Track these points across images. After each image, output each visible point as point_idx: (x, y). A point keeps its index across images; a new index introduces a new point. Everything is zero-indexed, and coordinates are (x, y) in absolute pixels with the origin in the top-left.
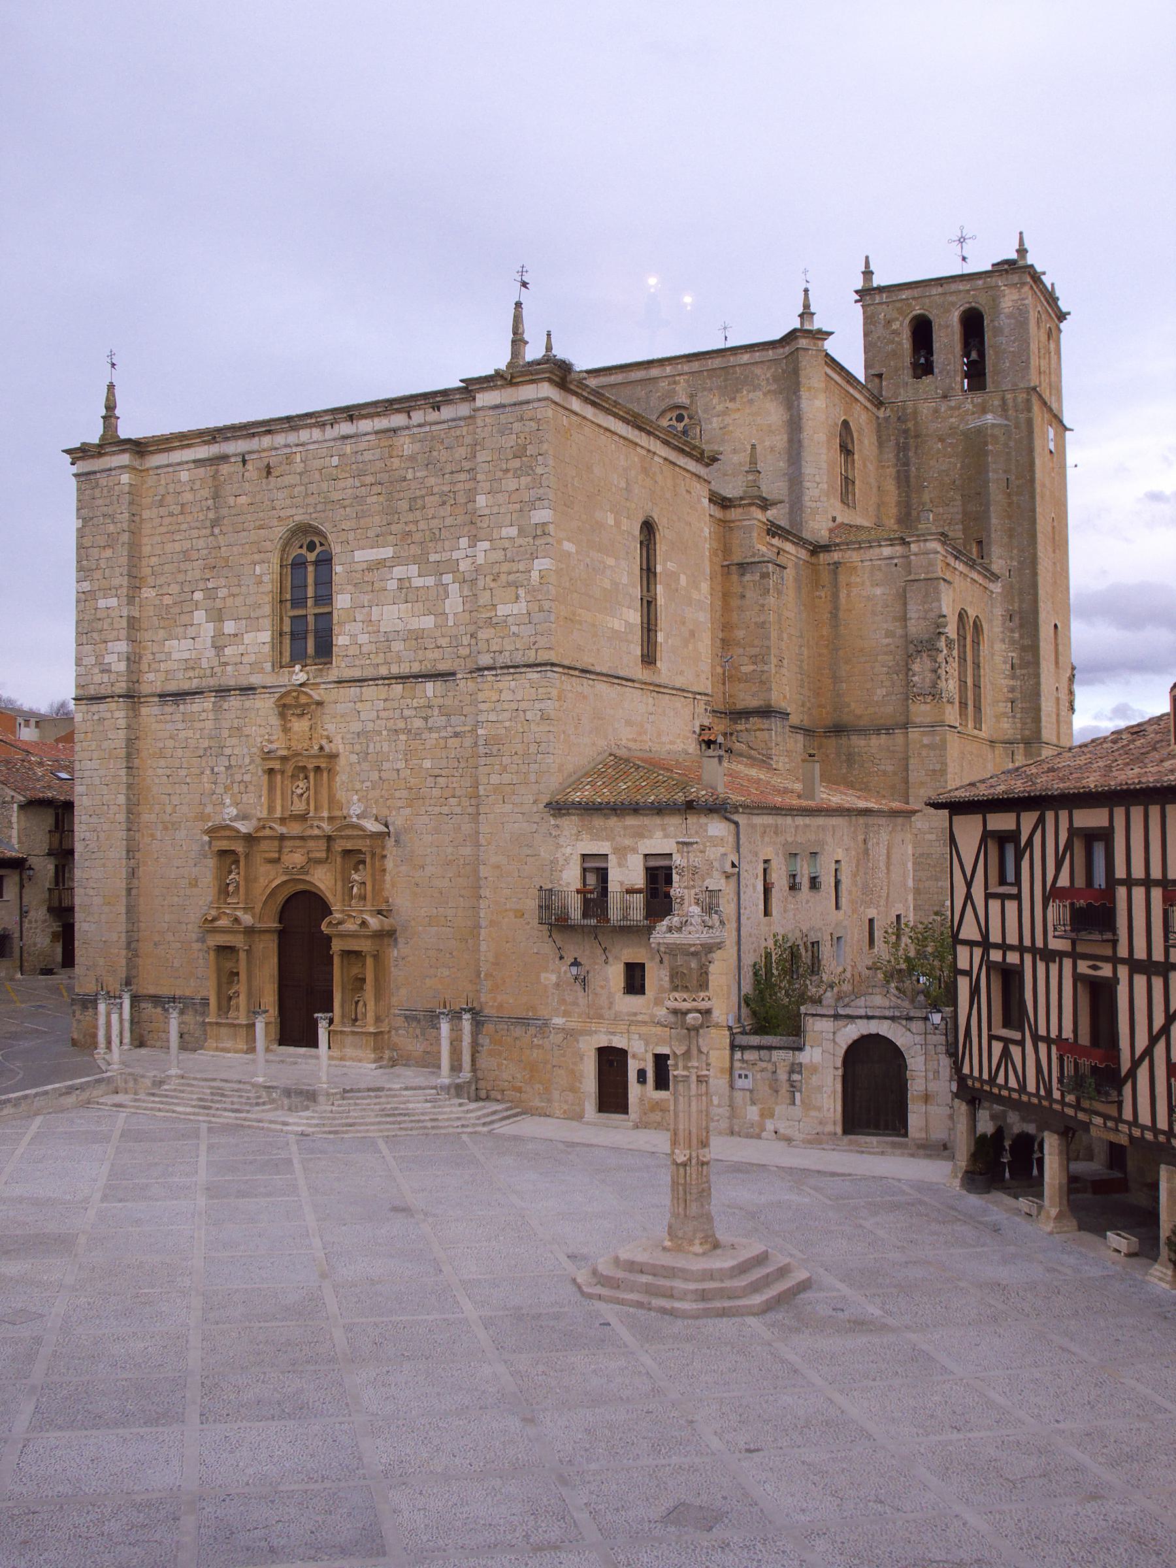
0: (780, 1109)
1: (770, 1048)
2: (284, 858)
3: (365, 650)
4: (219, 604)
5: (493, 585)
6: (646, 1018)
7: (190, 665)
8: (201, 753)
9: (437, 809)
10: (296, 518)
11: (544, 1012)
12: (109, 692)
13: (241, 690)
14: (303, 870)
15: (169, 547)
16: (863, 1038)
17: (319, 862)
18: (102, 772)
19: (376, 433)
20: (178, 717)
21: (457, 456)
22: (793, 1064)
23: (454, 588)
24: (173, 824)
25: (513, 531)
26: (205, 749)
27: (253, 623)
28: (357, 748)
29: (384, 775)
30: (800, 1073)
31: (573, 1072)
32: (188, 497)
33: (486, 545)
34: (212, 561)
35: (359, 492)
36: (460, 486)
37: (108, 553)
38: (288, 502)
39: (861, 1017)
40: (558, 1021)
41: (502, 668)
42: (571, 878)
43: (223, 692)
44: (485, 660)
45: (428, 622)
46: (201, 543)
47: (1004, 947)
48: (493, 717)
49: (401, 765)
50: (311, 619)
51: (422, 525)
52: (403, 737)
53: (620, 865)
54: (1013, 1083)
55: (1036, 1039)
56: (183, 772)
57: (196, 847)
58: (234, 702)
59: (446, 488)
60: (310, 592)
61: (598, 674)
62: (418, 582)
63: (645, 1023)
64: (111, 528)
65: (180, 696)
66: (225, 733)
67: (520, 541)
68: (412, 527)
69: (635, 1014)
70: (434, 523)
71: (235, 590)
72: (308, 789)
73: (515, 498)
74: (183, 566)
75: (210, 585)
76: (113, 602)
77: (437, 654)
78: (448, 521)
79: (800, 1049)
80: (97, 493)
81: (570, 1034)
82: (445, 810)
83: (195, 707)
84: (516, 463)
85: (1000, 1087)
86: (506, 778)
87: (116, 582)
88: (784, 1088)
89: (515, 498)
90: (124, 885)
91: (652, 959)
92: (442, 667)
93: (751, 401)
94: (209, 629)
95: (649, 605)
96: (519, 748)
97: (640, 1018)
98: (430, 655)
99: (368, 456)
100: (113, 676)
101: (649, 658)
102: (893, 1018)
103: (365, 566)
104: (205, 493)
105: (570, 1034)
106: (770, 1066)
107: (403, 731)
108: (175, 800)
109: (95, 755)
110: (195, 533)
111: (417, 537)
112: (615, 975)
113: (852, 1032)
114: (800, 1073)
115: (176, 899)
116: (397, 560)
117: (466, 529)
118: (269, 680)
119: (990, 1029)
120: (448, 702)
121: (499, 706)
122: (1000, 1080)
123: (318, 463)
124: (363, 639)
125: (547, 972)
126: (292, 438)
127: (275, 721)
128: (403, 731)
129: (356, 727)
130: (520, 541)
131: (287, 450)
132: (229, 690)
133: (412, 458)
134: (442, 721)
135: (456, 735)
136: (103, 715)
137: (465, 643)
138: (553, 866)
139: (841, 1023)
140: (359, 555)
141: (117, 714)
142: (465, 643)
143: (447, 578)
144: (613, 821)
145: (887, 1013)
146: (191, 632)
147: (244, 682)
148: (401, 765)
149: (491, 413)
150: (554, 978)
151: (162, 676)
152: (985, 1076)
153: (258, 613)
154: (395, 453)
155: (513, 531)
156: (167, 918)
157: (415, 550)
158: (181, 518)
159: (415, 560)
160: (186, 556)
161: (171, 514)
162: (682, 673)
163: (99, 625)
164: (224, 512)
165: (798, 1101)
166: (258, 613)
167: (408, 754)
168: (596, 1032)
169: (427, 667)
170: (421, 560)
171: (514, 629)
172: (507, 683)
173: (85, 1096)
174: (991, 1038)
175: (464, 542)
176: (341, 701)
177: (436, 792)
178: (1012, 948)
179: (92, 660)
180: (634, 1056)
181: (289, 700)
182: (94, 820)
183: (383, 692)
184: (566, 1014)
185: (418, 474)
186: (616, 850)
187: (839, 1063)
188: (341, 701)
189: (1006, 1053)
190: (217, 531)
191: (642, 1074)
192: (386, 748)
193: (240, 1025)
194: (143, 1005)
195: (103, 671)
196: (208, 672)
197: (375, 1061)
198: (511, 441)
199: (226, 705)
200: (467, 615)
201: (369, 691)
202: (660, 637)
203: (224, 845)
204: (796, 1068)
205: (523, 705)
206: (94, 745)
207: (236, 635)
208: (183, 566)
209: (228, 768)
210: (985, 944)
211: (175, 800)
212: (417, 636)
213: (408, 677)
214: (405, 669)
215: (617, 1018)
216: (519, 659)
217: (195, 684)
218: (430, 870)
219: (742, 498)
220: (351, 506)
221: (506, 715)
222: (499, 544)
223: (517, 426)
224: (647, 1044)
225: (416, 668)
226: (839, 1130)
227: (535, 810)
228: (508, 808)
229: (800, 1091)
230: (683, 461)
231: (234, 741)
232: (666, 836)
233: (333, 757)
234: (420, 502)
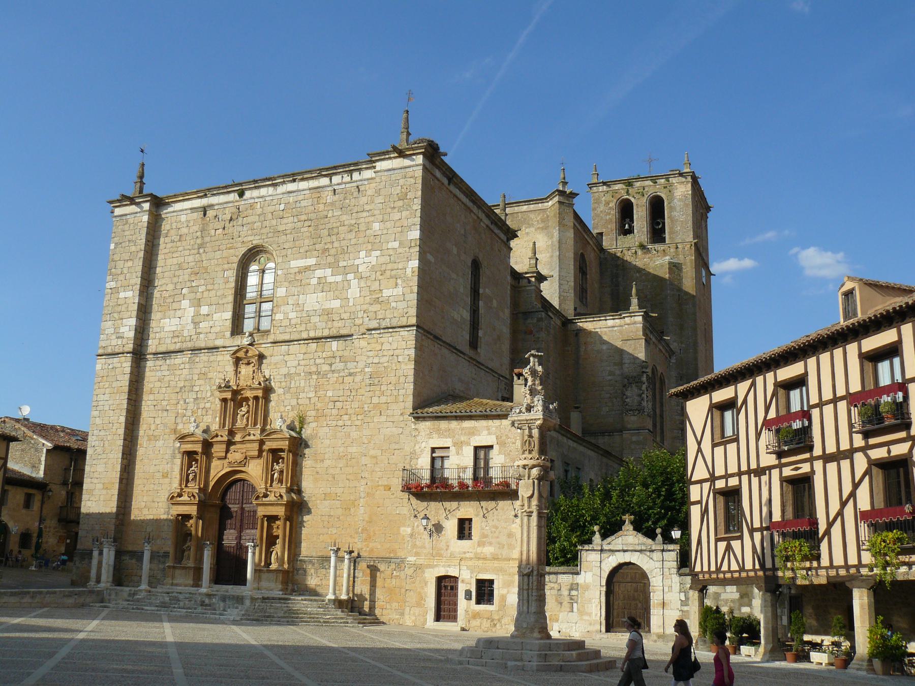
0: (562, 616)
1: (556, 573)
2: (229, 455)
3: (293, 322)
4: (199, 295)
5: (380, 277)
6: (472, 555)
7: (175, 335)
8: (178, 390)
9: (334, 423)
10: (254, 242)
11: (401, 554)
12: (121, 351)
13: (208, 349)
15: (169, 262)
16: (620, 566)
18: (110, 402)
19: (310, 189)
20: (165, 367)
21: (361, 203)
22: (572, 584)
23: (354, 283)
24: (155, 436)
25: (396, 244)
26: (181, 388)
28: (283, 384)
29: (300, 401)
30: (577, 590)
31: (420, 593)
32: (184, 231)
33: (378, 253)
34: (196, 270)
36: (362, 220)
37: (130, 264)
38: (250, 232)
39: (619, 551)
40: (411, 559)
41: (384, 329)
42: (423, 463)
43: (195, 350)
44: (374, 324)
45: (336, 304)
46: (191, 259)
48: (376, 360)
49: (312, 395)
51: (336, 244)
52: (315, 377)
53: (458, 454)
54: (735, 567)
55: (752, 531)
56: (164, 403)
57: (169, 451)
58: (203, 357)
59: (353, 222)
61: (444, 342)
62: (331, 279)
63: (471, 559)
64: (133, 249)
66: (196, 377)
67: (400, 250)
68: (329, 246)
69: (465, 553)
70: (344, 243)
71: (210, 287)
72: (248, 412)
73: (398, 224)
74: (177, 273)
75: (194, 284)
76: (129, 294)
77: (341, 324)
78: (353, 242)
79: (578, 574)
80: (126, 227)
81: (419, 568)
82: (340, 423)
84: (400, 203)
85: (724, 573)
86: (383, 399)
87: (132, 282)
88: (567, 599)
89: (398, 224)
90: (118, 476)
91: (477, 515)
92: (344, 332)
93: (527, 234)
95: (475, 312)
96: (394, 380)
97: (468, 555)
98: (336, 324)
99: (304, 203)
100: (125, 341)
101: (474, 343)
102: (641, 551)
103: (297, 270)
104: (196, 228)
105: (419, 568)
106: (556, 586)
107: (315, 373)
108: (158, 421)
110: (187, 253)
111: (333, 252)
112: (451, 527)
113: (612, 561)
114: (577, 590)
115: (152, 486)
116: (318, 266)
117: (365, 246)
118: (228, 342)
119: (716, 534)
120: (346, 353)
121: (380, 353)
122: (725, 567)
123: (271, 209)
124: (292, 315)
125: (405, 526)
126: (255, 193)
127: (230, 368)
128: (315, 373)
129: (284, 371)
130: (400, 250)
131: (252, 201)
132: (201, 350)
134: (341, 366)
135: (350, 374)
136: (115, 365)
137: (360, 316)
138: (414, 455)
139: (604, 555)
141: (124, 365)
142: (360, 316)
143: (350, 276)
144: (454, 424)
145: (639, 548)
146: (179, 313)
147: (211, 345)
148: (312, 395)
149: (386, 173)
150: (409, 530)
151: (156, 342)
152: (713, 568)
153: (225, 301)
154: (321, 201)
155: (396, 244)
156: (145, 499)
157: (331, 259)
158: (179, 244)
159: (330, 265)
160: (180, 267)
161: (173, 241)
162: (492, 360)
163: (119, 309)
164: (207, 239)
165: (575, 609)
166: (225, 301)
167: (317, 388)
168: (436, 566)
169: (334, 332)
170: (334, 266)
171: (394, 304)
173: (81, 600)
174: (717, 540)
175: (362, 254)
177: (335, 412)
178: (732, 475)
179: (112, 331)
180: (463, 581)
181: (241, 354)
182: (102, 433)
183: (303, 348)
184: (417, 554)
185: (335, 214)
186: (455, 444)
187: (604, 583)
189: (729, 548)
190: (201, 251)
191: (468, 594)
192: (302, 384)
193: (189, 568)
194: (124, 558)
195: (118, 338)
196: (188, 338)
197: (281, 590)
198: (398, 190)
199: (197, 360)
200: (362, 299)
201: (294, 348)
202: (481, 333)
204: (574, 587)
205: (396, 352)
207: (208, 315)
208: (177, 273)
210: (713, 478)
212: (328, 313)
213: (320, 338)
214: (319, 334)
215: (452, 556)
216: (395, 323)
217: (178, 347)
219: (526, 273)
220: (291, 233)
221: (385, 359)
222: (386, 252)
223: (401, 182)
224: (472, 573)
226: (603, 629)
227: (401, 419)
228: (383, 418)
229: (577, 602)
230: (497, 231)
231: (201, 382)
232: (489, 434)
234: (335, 230)
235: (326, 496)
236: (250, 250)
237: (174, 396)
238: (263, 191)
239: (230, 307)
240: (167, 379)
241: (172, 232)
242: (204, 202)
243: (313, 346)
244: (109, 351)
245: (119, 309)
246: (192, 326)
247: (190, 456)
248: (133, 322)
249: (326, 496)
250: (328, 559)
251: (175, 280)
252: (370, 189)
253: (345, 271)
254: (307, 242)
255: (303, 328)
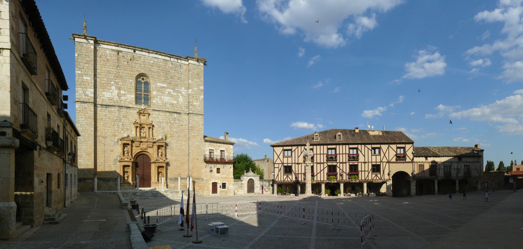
2: (141, 146)
7: (110, 99)
12: (88, 101)
14: (146, 149)
15: (103, 69)
17: (150, 147)
18: (86, 121)
25: (196, 89)
27: (129, 93)
32: (109, 58)
35: (159, 71)
37: (87, 65)
42: (207, 153)
43: (121, 107)
45: (175, 102)
46: (114, 70)
47: (288, 163)
49: (169, 129)
50: (143, 95)
51: (174, 82)
58: (124, 110)
60: (143, 89)
64: (88, 59)
65: (107, 106)
71: (124, 84)
76: (89, 78)
77: (177, 109)
80: (83, 48)
81: (207, 180)
83: (112, 109)
84: (197, 76)
86: (195, 134)
94: (116, 92)
99: (161, 64)
105: (207, 180)
108: (106, 131)
109: (83, 117)
110: (112, 67)
116: (168, 88)
124: (159, 102)
127: (137, 116)
129: (158, 120)
133: (171, 68)
134: (178, 122)
140: (158, 84)
143: (179, 94)
146: (110, 91)
148: (169, 129)
155: (196, 89)
157: (172, 87)
160: (109, 72)
163: (84, 83)
167: (170, 127)
169: (175, 111)
170: (174, 89)
172: (195, 117)
175: (183, 88)
176: (154, 114)
183: (164, 114)
188: (154, 114)
189: (287, 176)
198: (196, 72)
201: (161, 113)
203: (126, 142)
206: (83, 114)
209: (123, 125)
210: (283, 163)
211: (106, 131)
212: (172, 104)
216: (197, 113)
217: (112, 104)
218: (175, 151)
225: (172, 111)
233: (153, 126)
235: (175, 160)
236: (140, 74)
237: (113, 122)
238: (144, 53)
239: (134, 93)
240: (108, 115)
241: (103, 57)
242: (117, 48)
243: (168, 114)
244: (82, 100)
245: (84, 83)
246: (117, 97)
247: (125, 145)
248: (93, 90)
249: (175, 160)
250: (177, 179)
251: (107, 77)
252: (185, 67)
253: (178, 92)
254: (163, 78)
255: (164, 107)
